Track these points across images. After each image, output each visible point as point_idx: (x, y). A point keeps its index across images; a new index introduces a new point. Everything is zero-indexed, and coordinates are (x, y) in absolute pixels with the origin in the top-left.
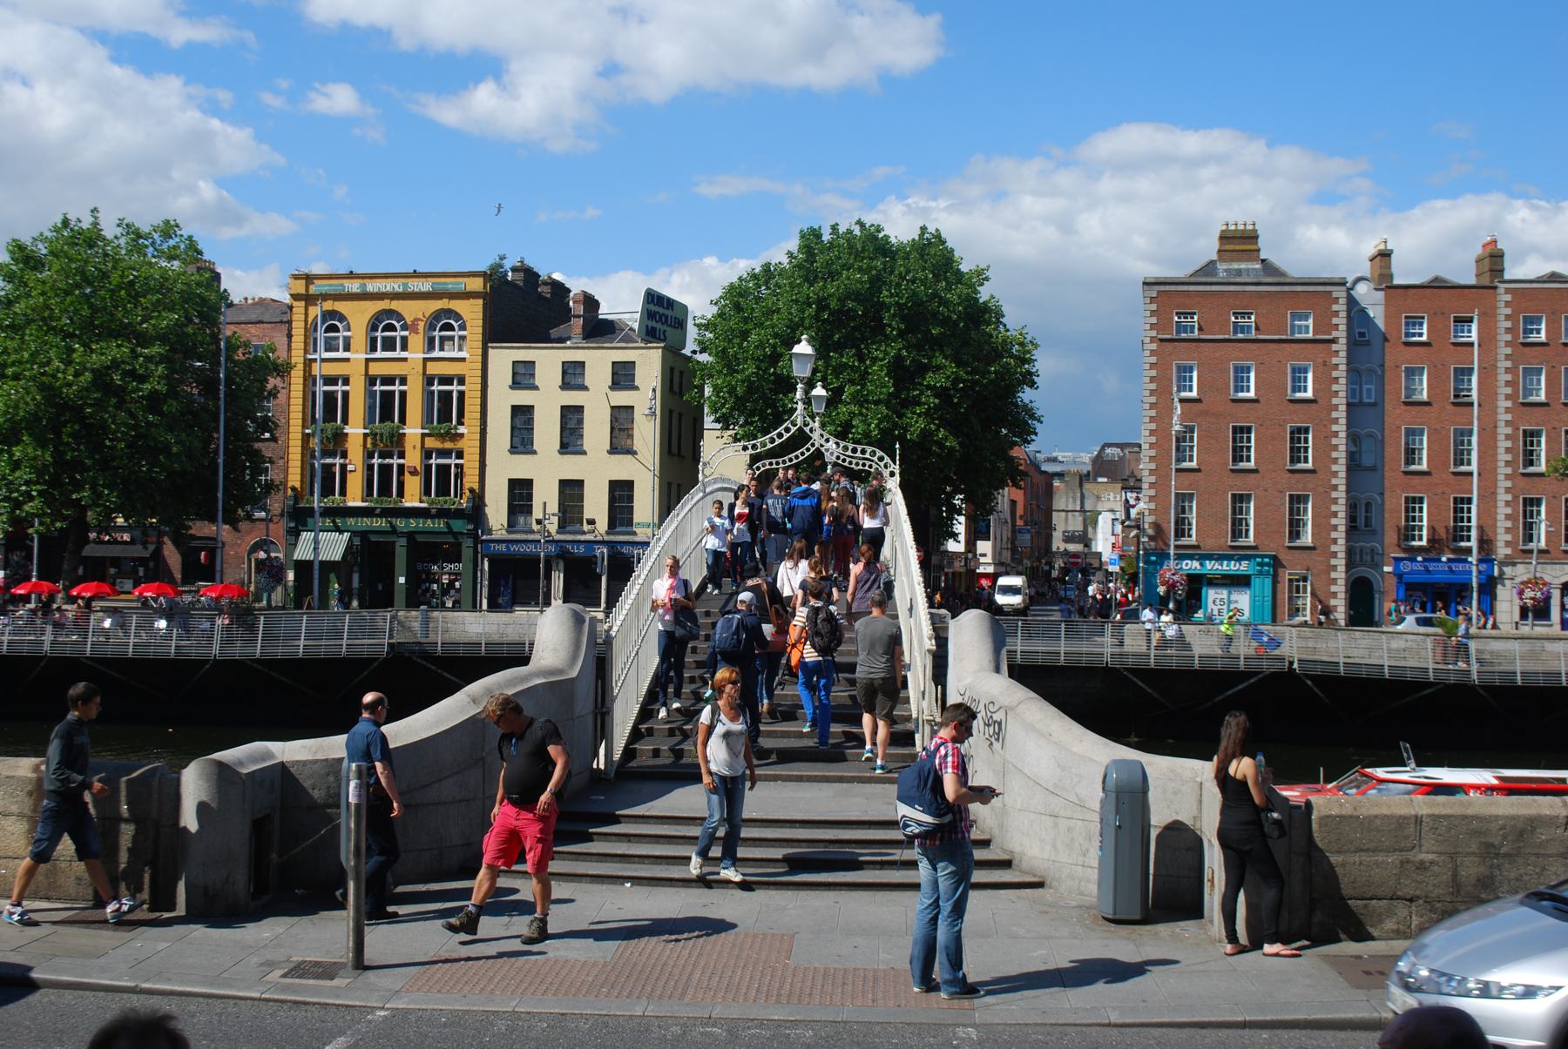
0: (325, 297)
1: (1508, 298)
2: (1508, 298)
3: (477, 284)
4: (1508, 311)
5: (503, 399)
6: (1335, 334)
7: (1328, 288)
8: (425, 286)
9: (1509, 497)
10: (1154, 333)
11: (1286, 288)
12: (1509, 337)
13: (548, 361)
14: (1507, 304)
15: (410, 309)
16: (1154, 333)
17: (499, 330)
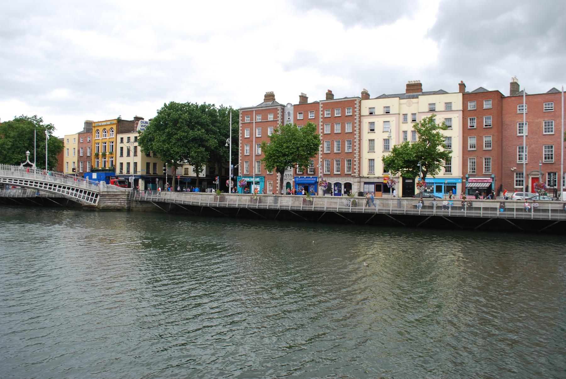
0: (96, 126)
1: (322, 105)
2: (322, 105)
3: (115, 122)
4: (322, 109)
5: (119, 145)
6: (278, 119)
7: (277, 107)
8: (109, 123)
9: (321, 160)
11: (268, 108)
12: (322, 116)
13: (125, 136)
14: (322, 107)
15: (106, 128)
17: (119, 132)
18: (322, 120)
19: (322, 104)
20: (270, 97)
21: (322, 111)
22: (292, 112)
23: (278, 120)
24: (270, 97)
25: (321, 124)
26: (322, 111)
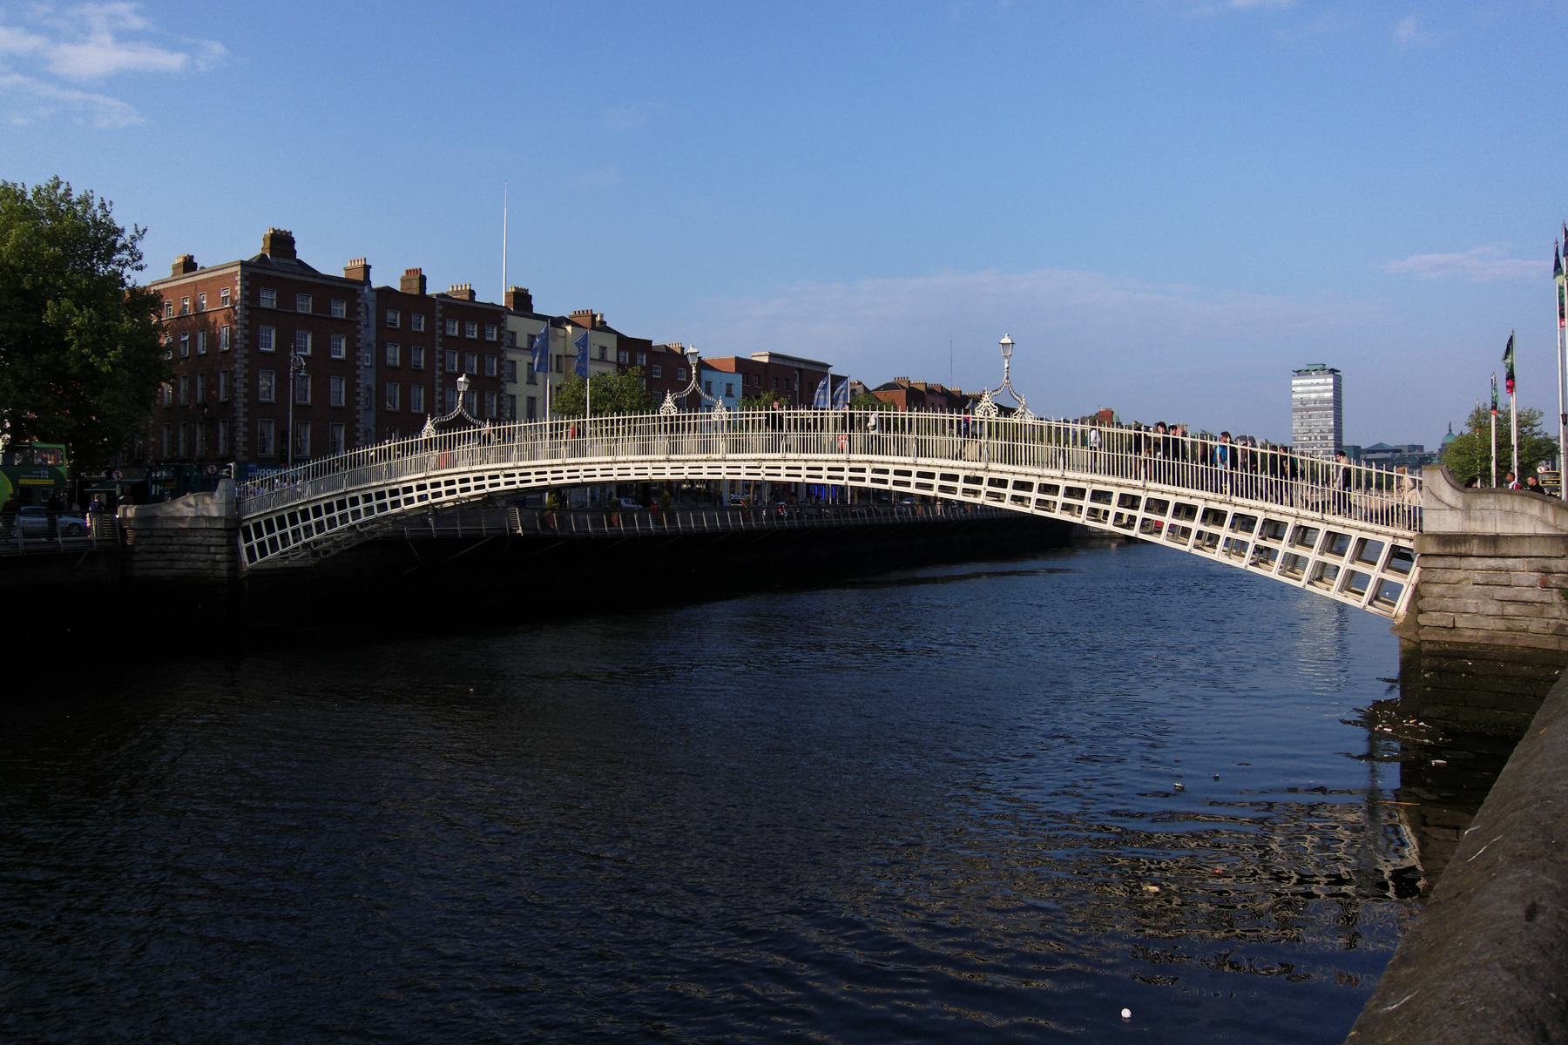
1: (441, 307)
2: (441, 307)
6: (359, 318)
10: (247, 303)
16: (247, 303)
18: (440, 340)
19: (441, 303)
20: (281, 243)
21: (441, 319)
22: (372, 306)
23: (359, 323)
24: (281, 243)
25: (439, 348)
26: (441, 319)
